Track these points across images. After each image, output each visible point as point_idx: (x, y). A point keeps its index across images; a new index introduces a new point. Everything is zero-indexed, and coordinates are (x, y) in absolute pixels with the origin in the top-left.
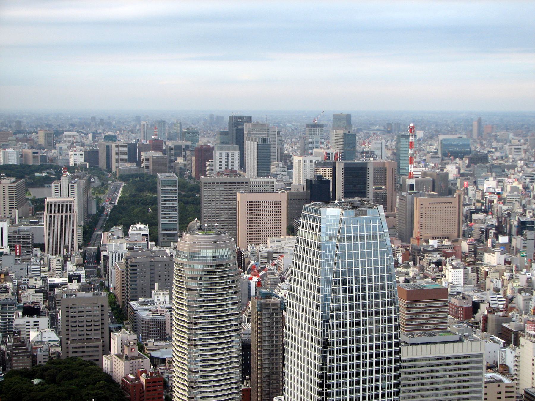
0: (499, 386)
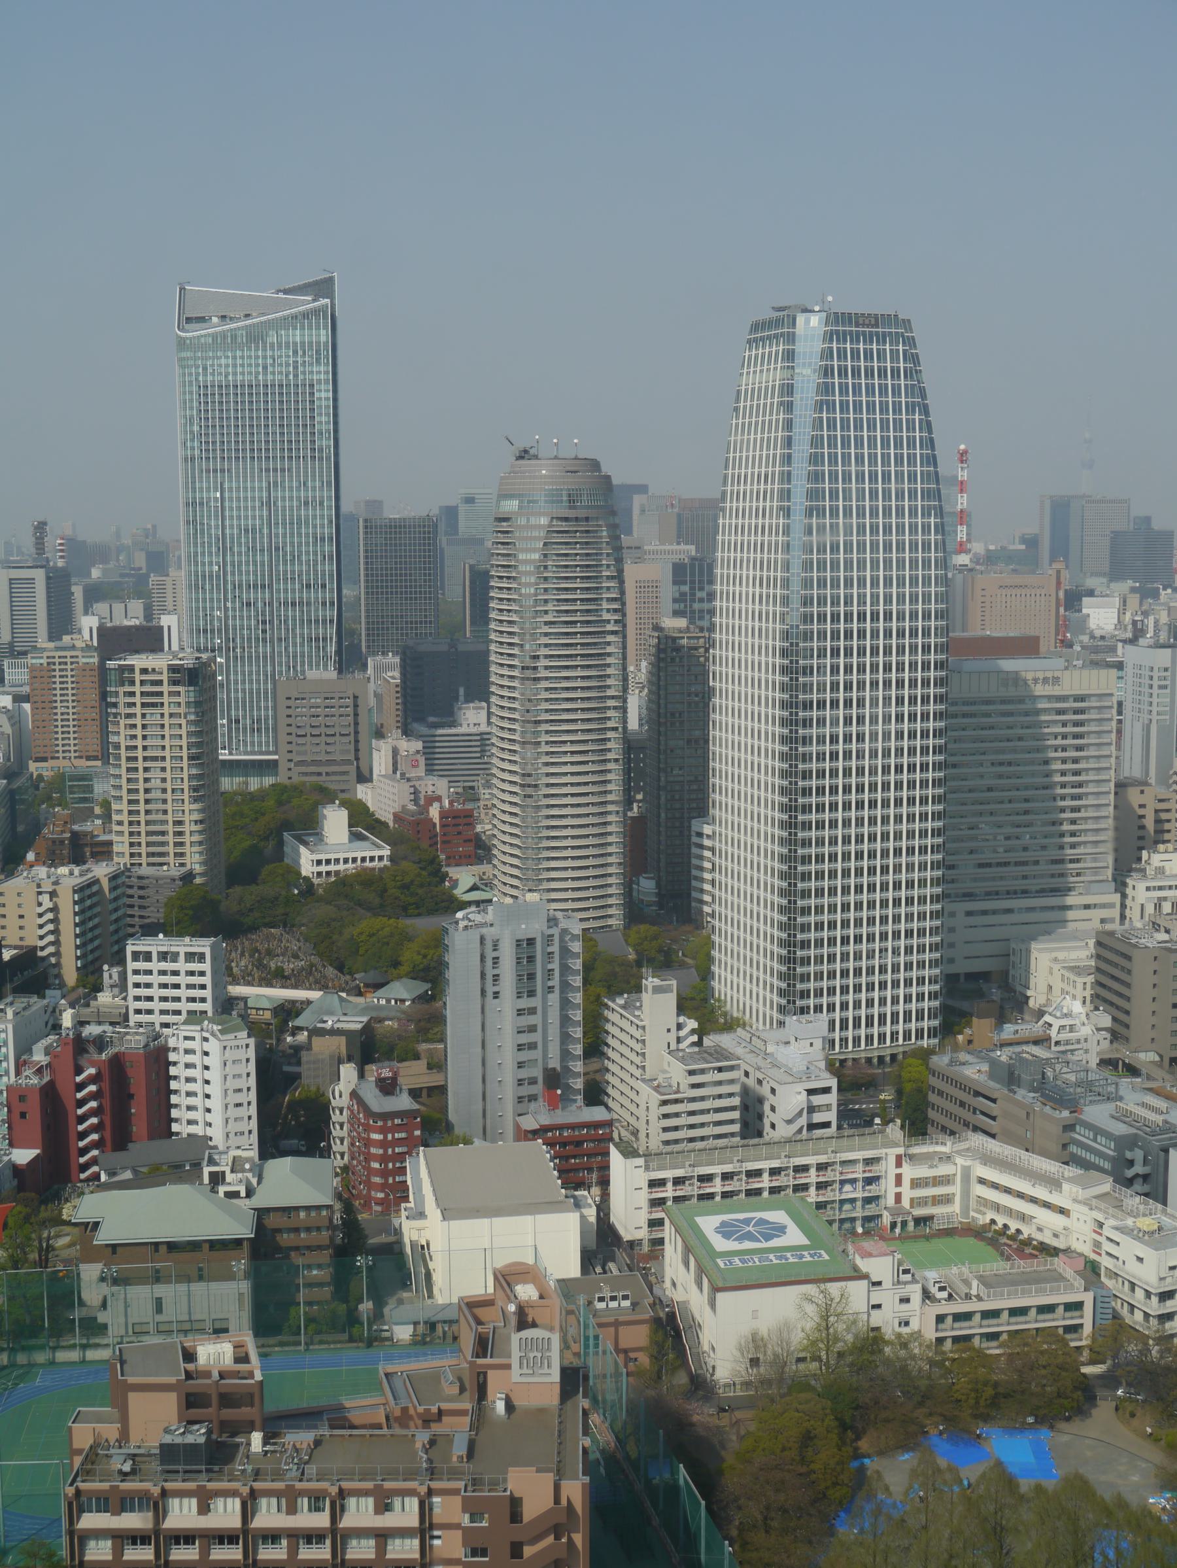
0: (1142, 792)
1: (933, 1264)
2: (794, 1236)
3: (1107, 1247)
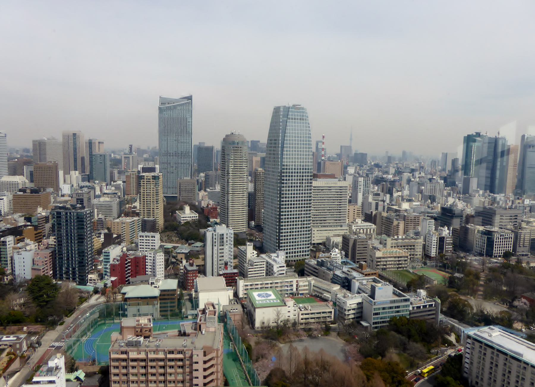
1: (300, 303)
2: (273, 297)
3: (337, 300)
